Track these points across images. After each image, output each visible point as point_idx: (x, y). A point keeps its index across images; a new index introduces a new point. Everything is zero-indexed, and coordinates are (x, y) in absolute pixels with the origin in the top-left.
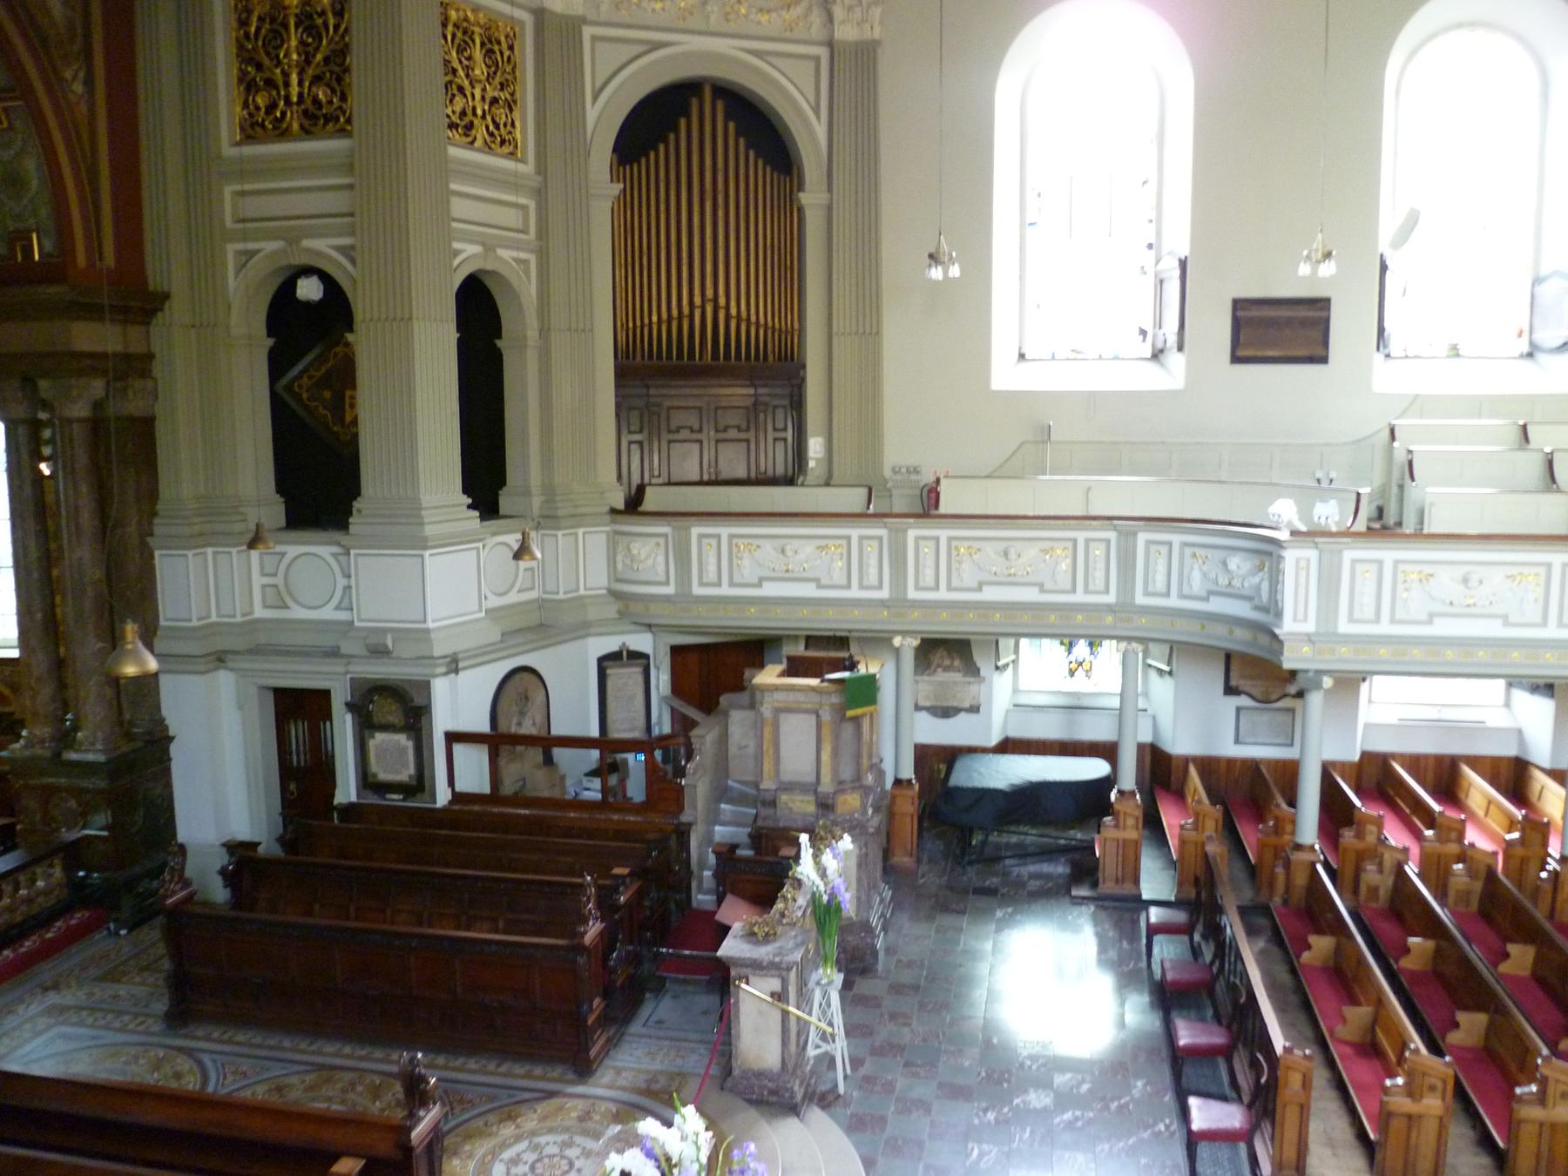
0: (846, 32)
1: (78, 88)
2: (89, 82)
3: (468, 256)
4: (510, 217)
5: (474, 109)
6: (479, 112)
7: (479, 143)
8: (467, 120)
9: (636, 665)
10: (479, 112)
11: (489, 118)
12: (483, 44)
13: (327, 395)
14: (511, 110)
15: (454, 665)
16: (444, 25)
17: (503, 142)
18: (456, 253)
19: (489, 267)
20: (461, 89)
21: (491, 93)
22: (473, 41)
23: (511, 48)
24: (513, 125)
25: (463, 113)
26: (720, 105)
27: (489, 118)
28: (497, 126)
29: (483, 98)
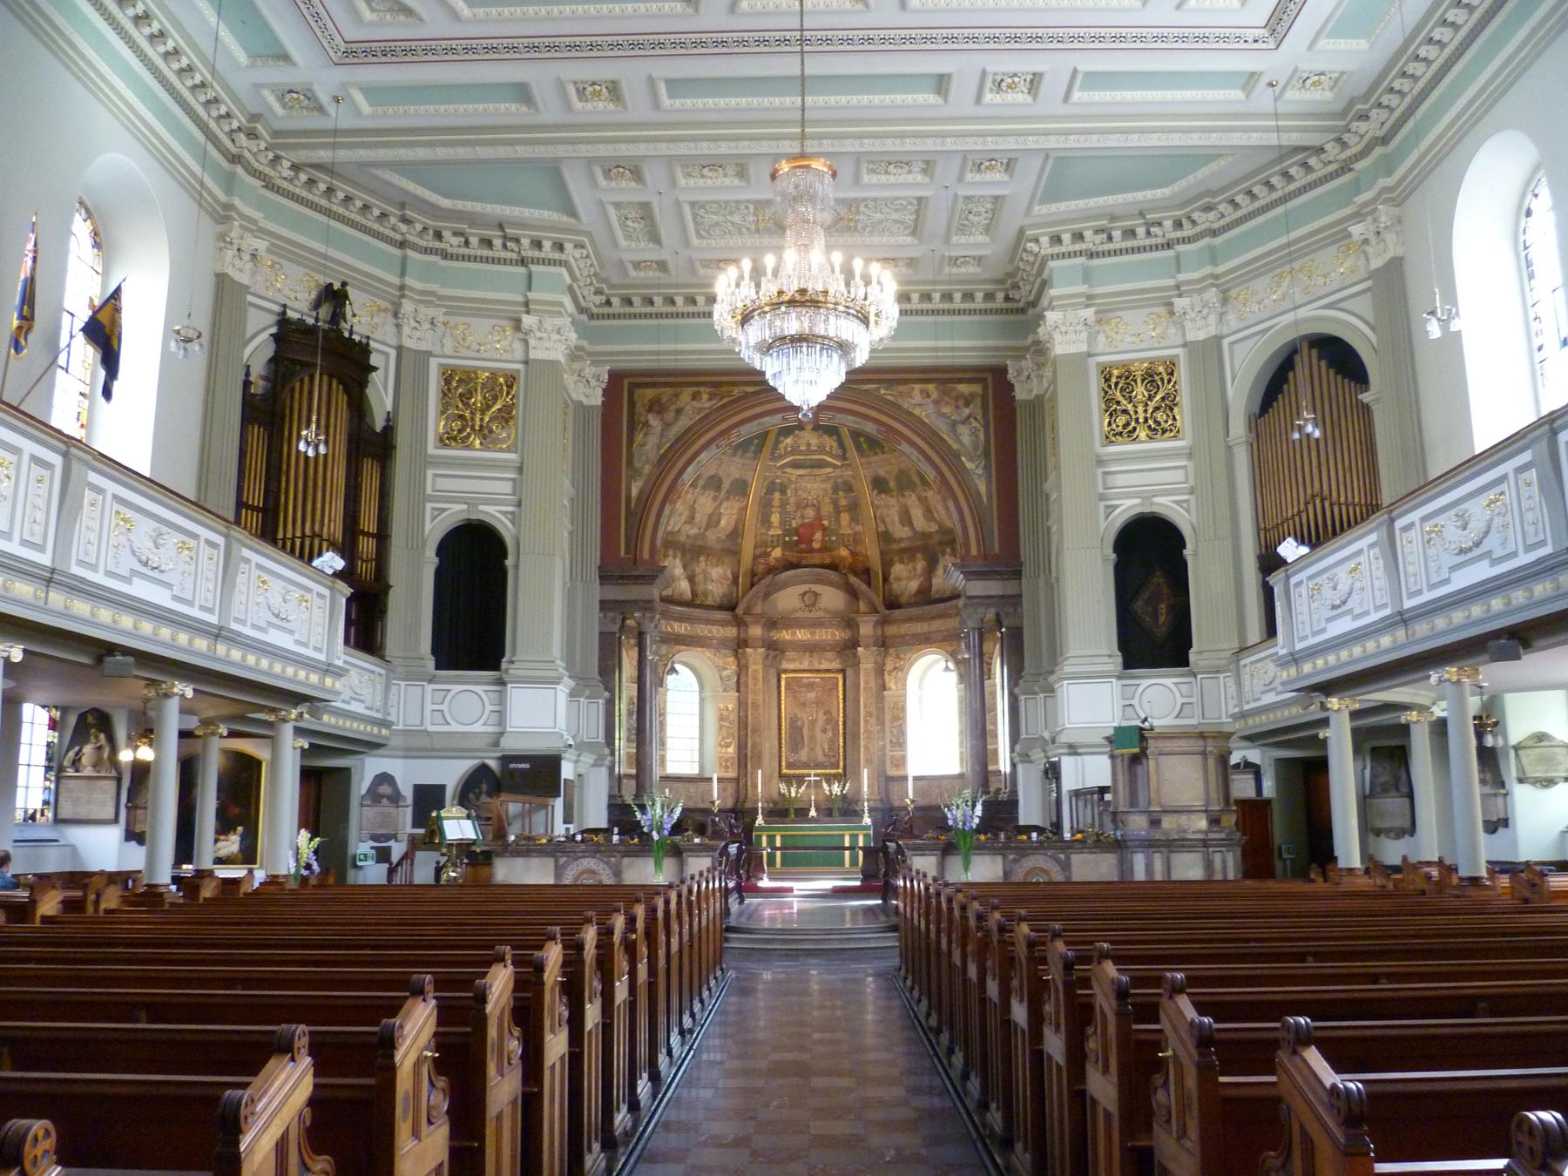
0: (1376, 263)
1: (980, 471)
2: (987, 467)
3: (1127, 508)
4: (1178, 476)
5: (1137, 420)
6: (1141, 420)
7: (1143, 435)
8: (1130, 428)
9: (1249, 773)
10: (1141, 420)
11: (1151, 422)
12: (1143, 381)
13: (1150, 609)
14: (1172, 410)
15: (1073, 750)
16: (1107, 380)
17: (1164, 431)
18: (1116, 507)
19: (1147, 510)
20: (1125, 412)
21: (1152, 405)
22: (1135, 381)
23: (1172, 374)
24: (1174, 419)
25: (1128, 424)
26: (1314, 352)
27: (1151, 422)
28: (1159, 424)
29: (1146, 411)
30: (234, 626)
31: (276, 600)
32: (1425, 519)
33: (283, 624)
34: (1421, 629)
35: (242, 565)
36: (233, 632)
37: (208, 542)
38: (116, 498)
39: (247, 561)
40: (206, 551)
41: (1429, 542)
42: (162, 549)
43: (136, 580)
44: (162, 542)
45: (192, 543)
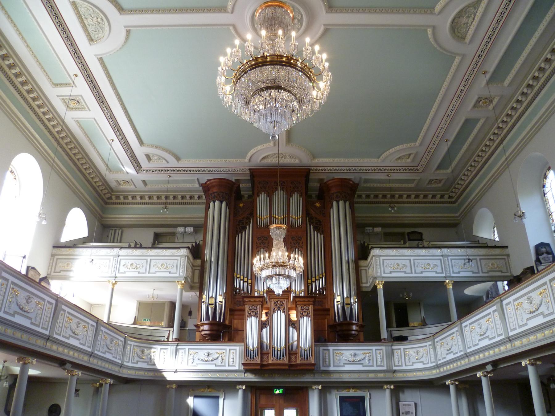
30: (55, 336)
31: (74, 326)
32: (515, 300)
33: (76, 336)
34: (517, 343)
35: (62, 312)
36: (55, 338)
37: (49, 302)
38: (13, 283)
39: (64, 311)
40: (48, 305)
41: (517, 309)
42: (30, 304)
43: (16, 316)
44: (30, 301)
45: (42, 302)
